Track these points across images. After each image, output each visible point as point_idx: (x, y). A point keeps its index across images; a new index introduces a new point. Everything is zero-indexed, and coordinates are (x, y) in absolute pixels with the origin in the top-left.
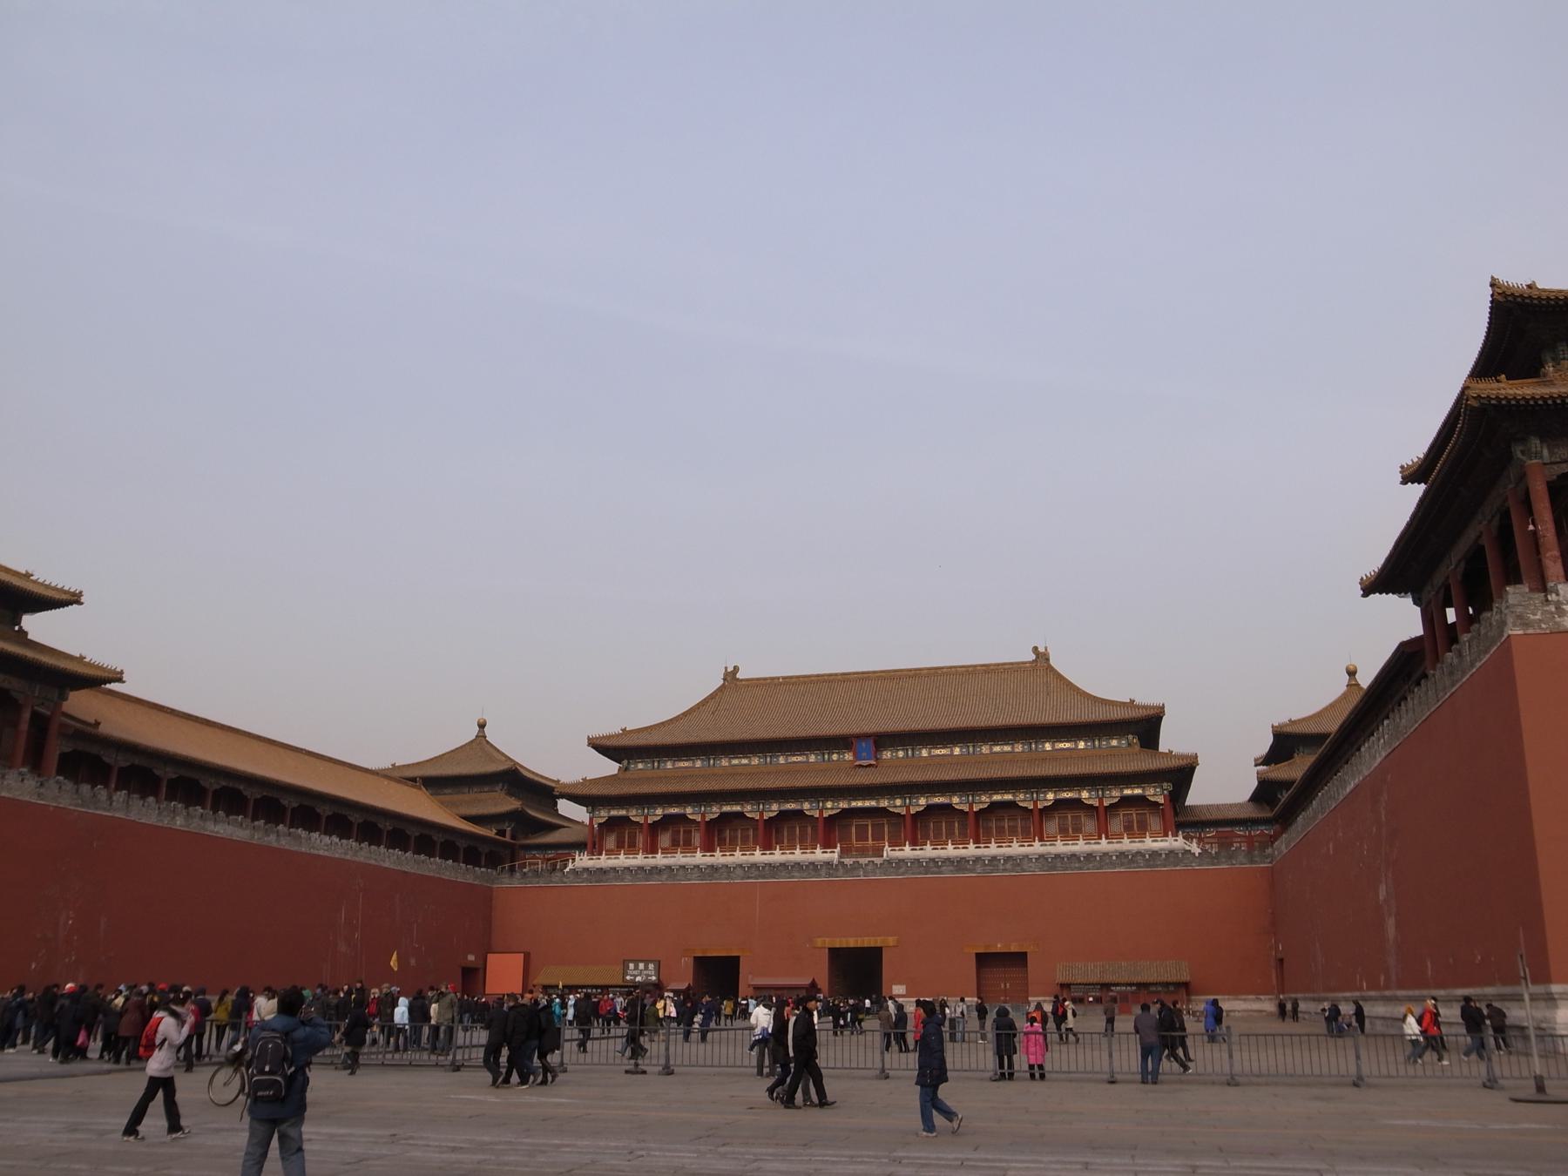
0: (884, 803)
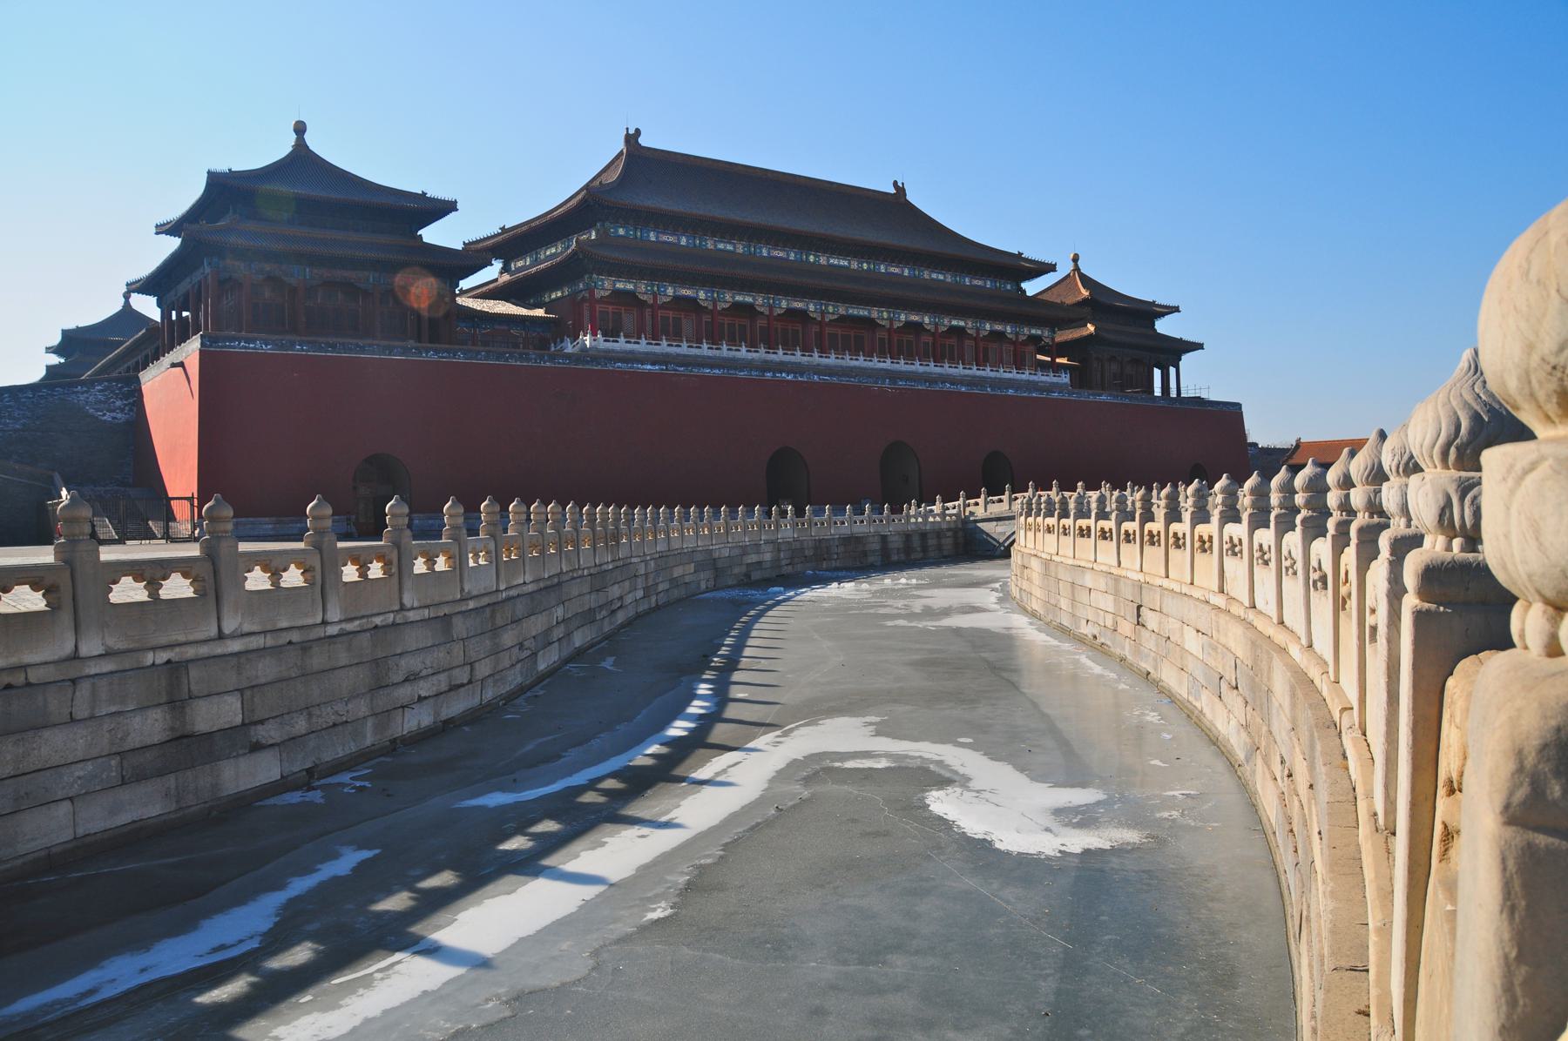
0: (875, 315)
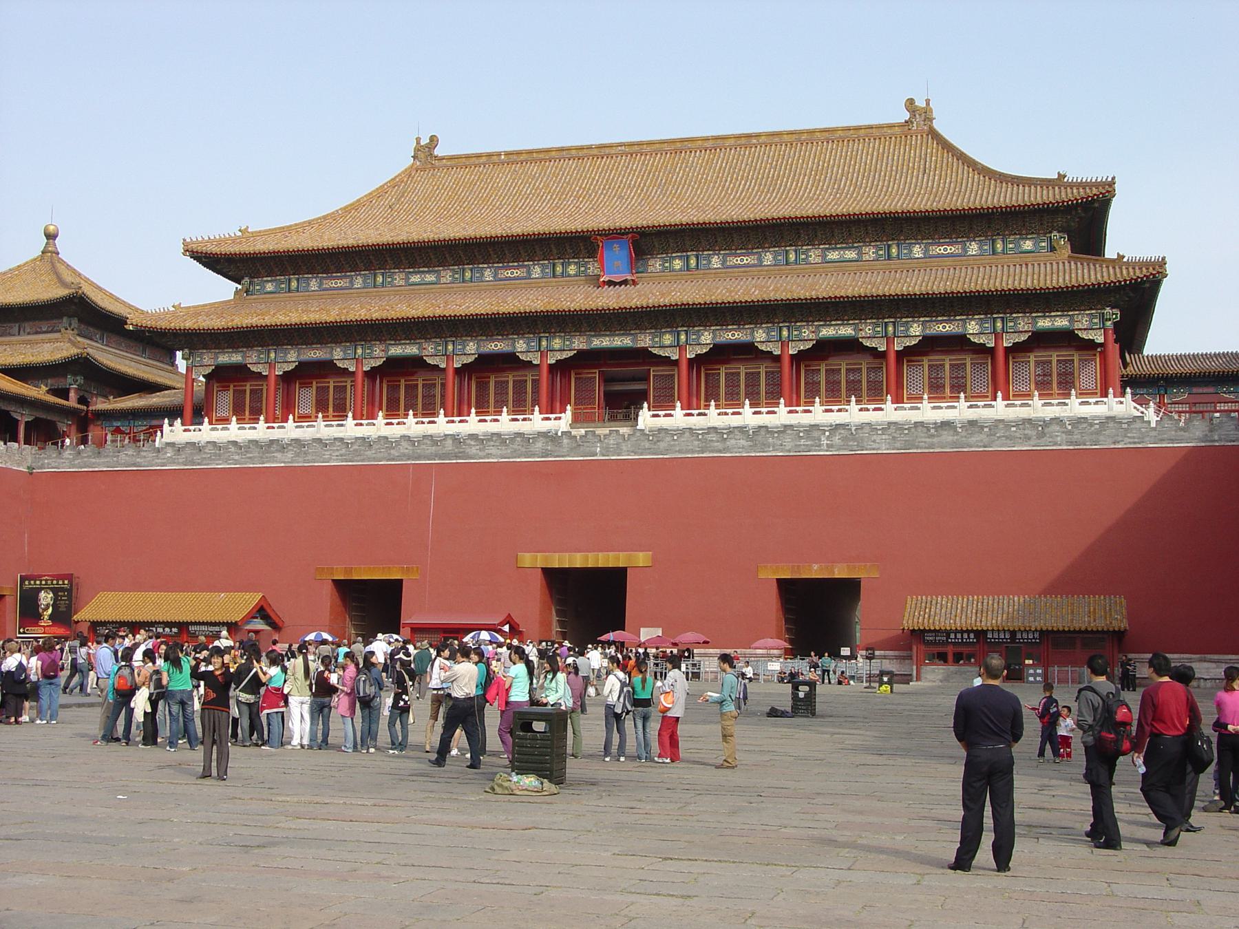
0: (644, 341)
